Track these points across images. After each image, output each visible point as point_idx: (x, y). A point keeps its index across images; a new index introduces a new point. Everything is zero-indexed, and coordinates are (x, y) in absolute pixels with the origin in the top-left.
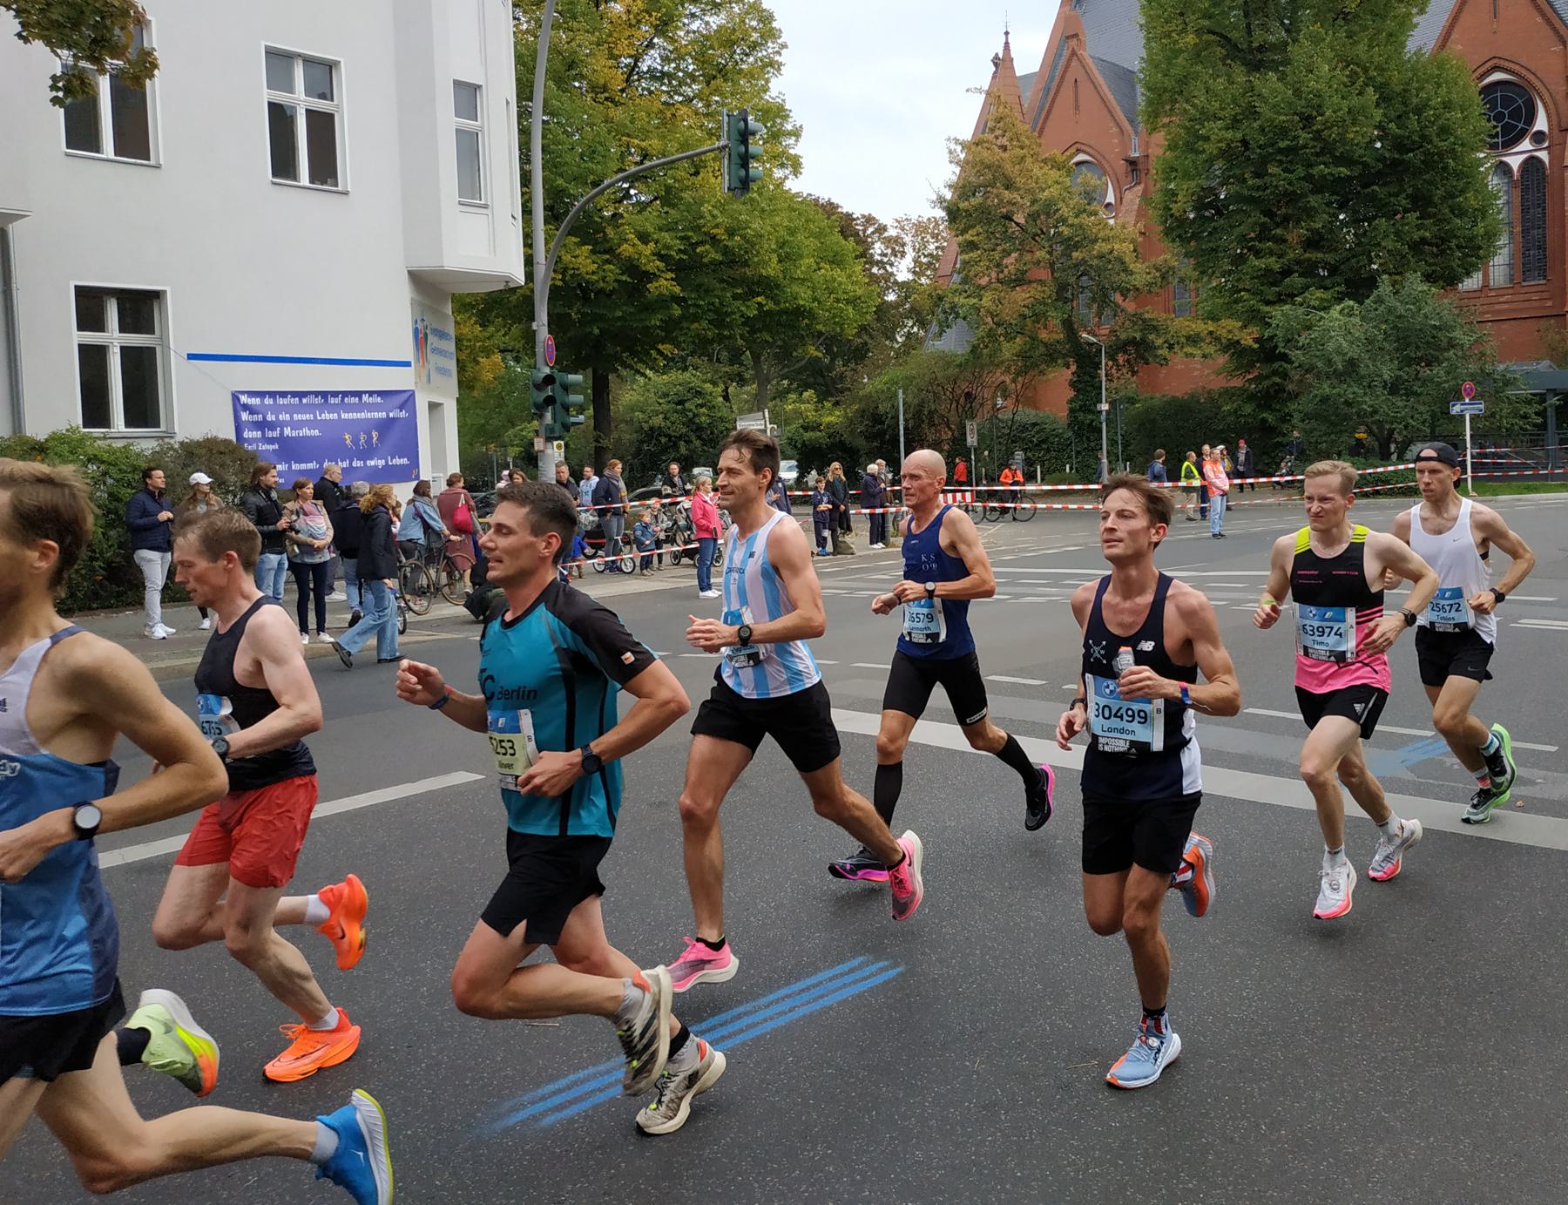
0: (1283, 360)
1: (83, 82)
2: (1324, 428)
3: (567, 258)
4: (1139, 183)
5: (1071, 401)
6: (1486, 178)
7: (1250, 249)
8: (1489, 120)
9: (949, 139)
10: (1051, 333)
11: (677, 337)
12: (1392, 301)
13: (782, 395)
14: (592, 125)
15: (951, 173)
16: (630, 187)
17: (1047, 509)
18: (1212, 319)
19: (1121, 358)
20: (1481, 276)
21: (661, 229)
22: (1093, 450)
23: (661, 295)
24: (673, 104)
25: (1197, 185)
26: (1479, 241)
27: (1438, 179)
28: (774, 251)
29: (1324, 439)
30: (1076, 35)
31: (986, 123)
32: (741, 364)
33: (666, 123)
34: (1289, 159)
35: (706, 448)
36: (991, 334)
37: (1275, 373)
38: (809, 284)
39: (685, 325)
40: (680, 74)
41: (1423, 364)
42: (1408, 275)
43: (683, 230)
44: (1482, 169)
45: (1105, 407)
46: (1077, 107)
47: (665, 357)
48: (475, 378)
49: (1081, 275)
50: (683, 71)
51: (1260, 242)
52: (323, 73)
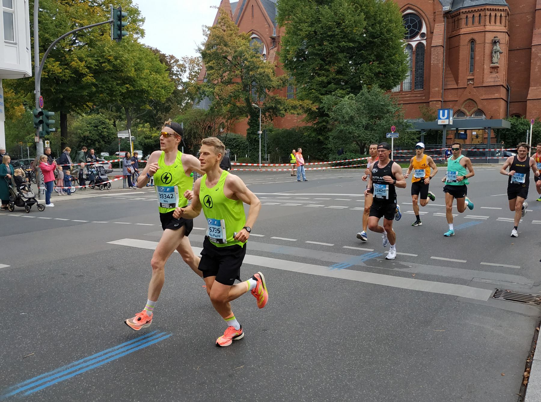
0: (327, 117)
2: (340, 142)
3: (50, 66)
4: (276, 47)
5: (248, 130)
6: (402, 50)
7: (316, 73)
8: (405, 28)
9: (203, 26)
10: (241, 103)
11: (94, 99)
12: (367, 95)
13: (136, 125)
14: (60, 13)
15: (204, 39)
16: (76, 39)
17: (237, 171)
18: (301, 100)
19: (267, 114)
20: (400, 87)
21: (88, 56)
22: (256, 149)
23: (88, 82)
24: (94, 7)
26: (400, 73)
27: (386, 49)
28: (133, 67)
29: (340, 146)
31: (218, 21)
32: (121, 112)
33: (91, 14)
34: (332, 39)
36: (218, 103)
37: (324, 121)
38: (147, 80)
41: (377, 119)
42: (373, 85)
43: (97, 57)
44: (402, 46)
45: (260, 132)
46: (253, 16)
47: (90, 109)
48: (13, 114)
49: (253, 81)
51: (320, 71)
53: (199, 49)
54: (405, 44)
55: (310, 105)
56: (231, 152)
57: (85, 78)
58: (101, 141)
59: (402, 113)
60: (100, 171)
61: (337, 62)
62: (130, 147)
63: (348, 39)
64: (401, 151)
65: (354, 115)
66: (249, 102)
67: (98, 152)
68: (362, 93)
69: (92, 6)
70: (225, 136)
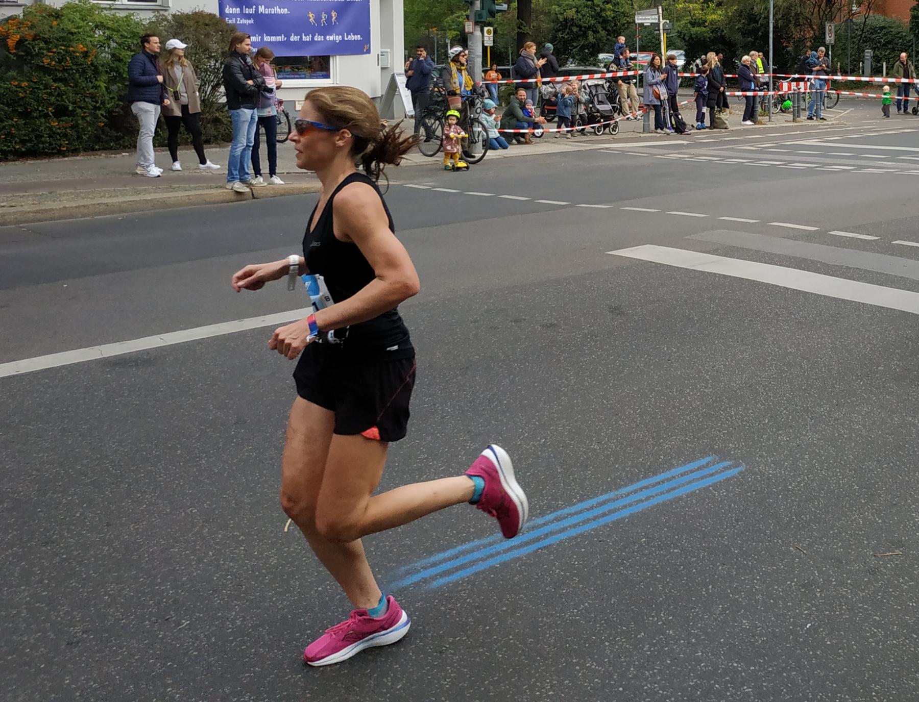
5: (914, 9)
35: (610, 38)
56: (874, 57)
60: (597, 95)
62: (660, 43)
70: (864, 20)
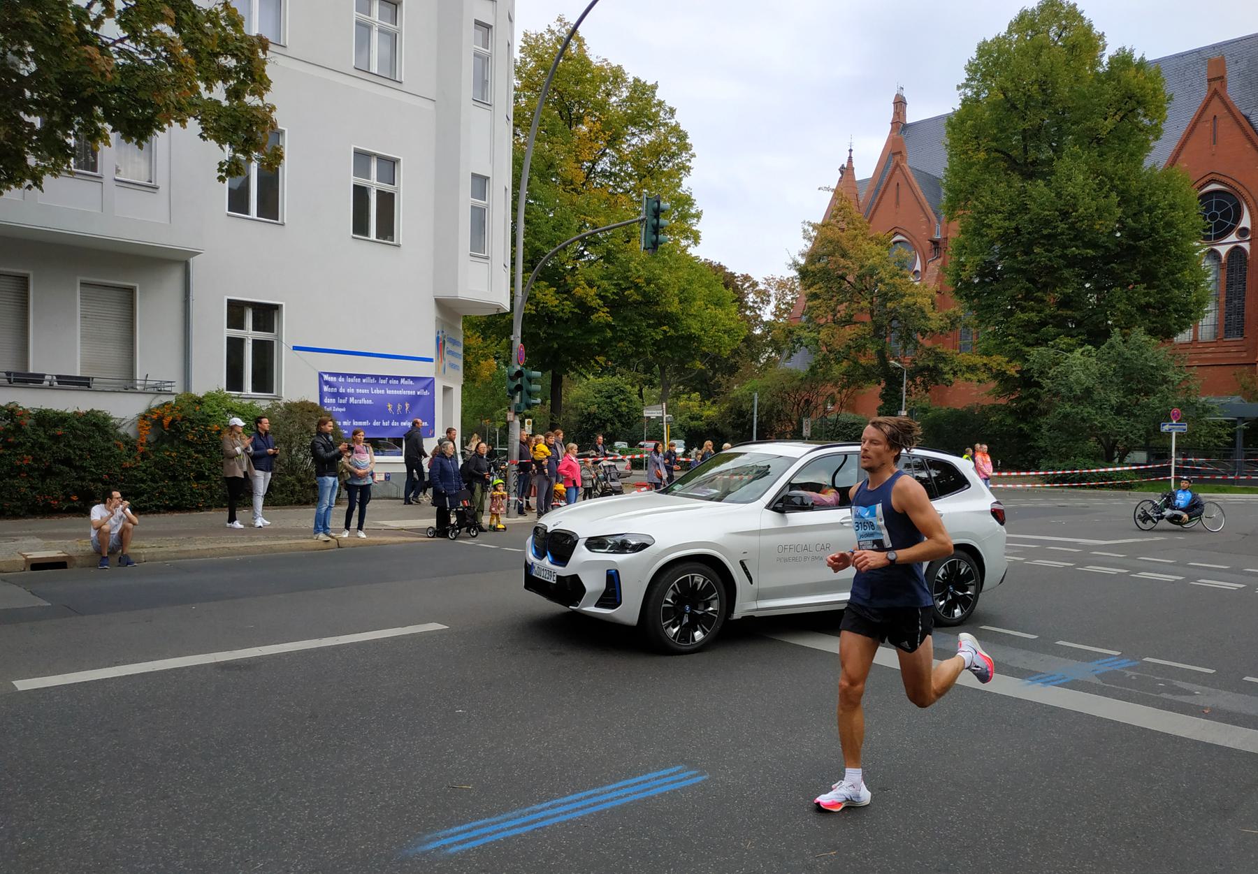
1: (238, 168)
3: (539, 295)
7: (1017, 306)
8: (1205, 219)
9: (804, 222)
10: (869, 359)
12: (1122, 348)
13: (677, 396)
15: (806, 246)
18: (987, 355)
19: (918, 380)
20: (1192, 333)
21: (602, 279)
23: (599, 323)
25: (981, 259)
26: (1191, 307)
28: (677, 295)
30: (900, 152)
32: (652, 373)
36: (825, 359)
37: (1031, 395)
39: (614, 344)
40: (623, 174)
41: (1142, 394)
42: (1135, 329)
46: (897, 203)
50: (624, 172)
52: (389, 166)
53: (795, 264)
54: (1202, 251)
55: (1004, 365)
57: (596, 315)
58: (616, 421)
59: (1195, 384)
61: (1059, 285)
63: (1083, 242)
64: (1193, 459)
65: (1094, 385)
66: (884, 357)
67: (610, 440)
68: (1111, 344)
69: (614, 194)
